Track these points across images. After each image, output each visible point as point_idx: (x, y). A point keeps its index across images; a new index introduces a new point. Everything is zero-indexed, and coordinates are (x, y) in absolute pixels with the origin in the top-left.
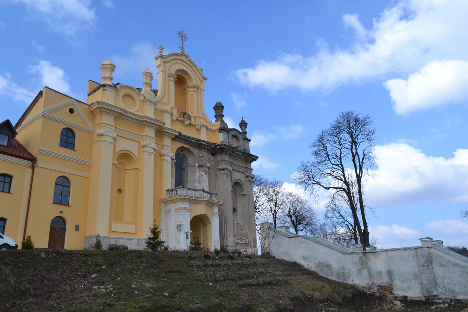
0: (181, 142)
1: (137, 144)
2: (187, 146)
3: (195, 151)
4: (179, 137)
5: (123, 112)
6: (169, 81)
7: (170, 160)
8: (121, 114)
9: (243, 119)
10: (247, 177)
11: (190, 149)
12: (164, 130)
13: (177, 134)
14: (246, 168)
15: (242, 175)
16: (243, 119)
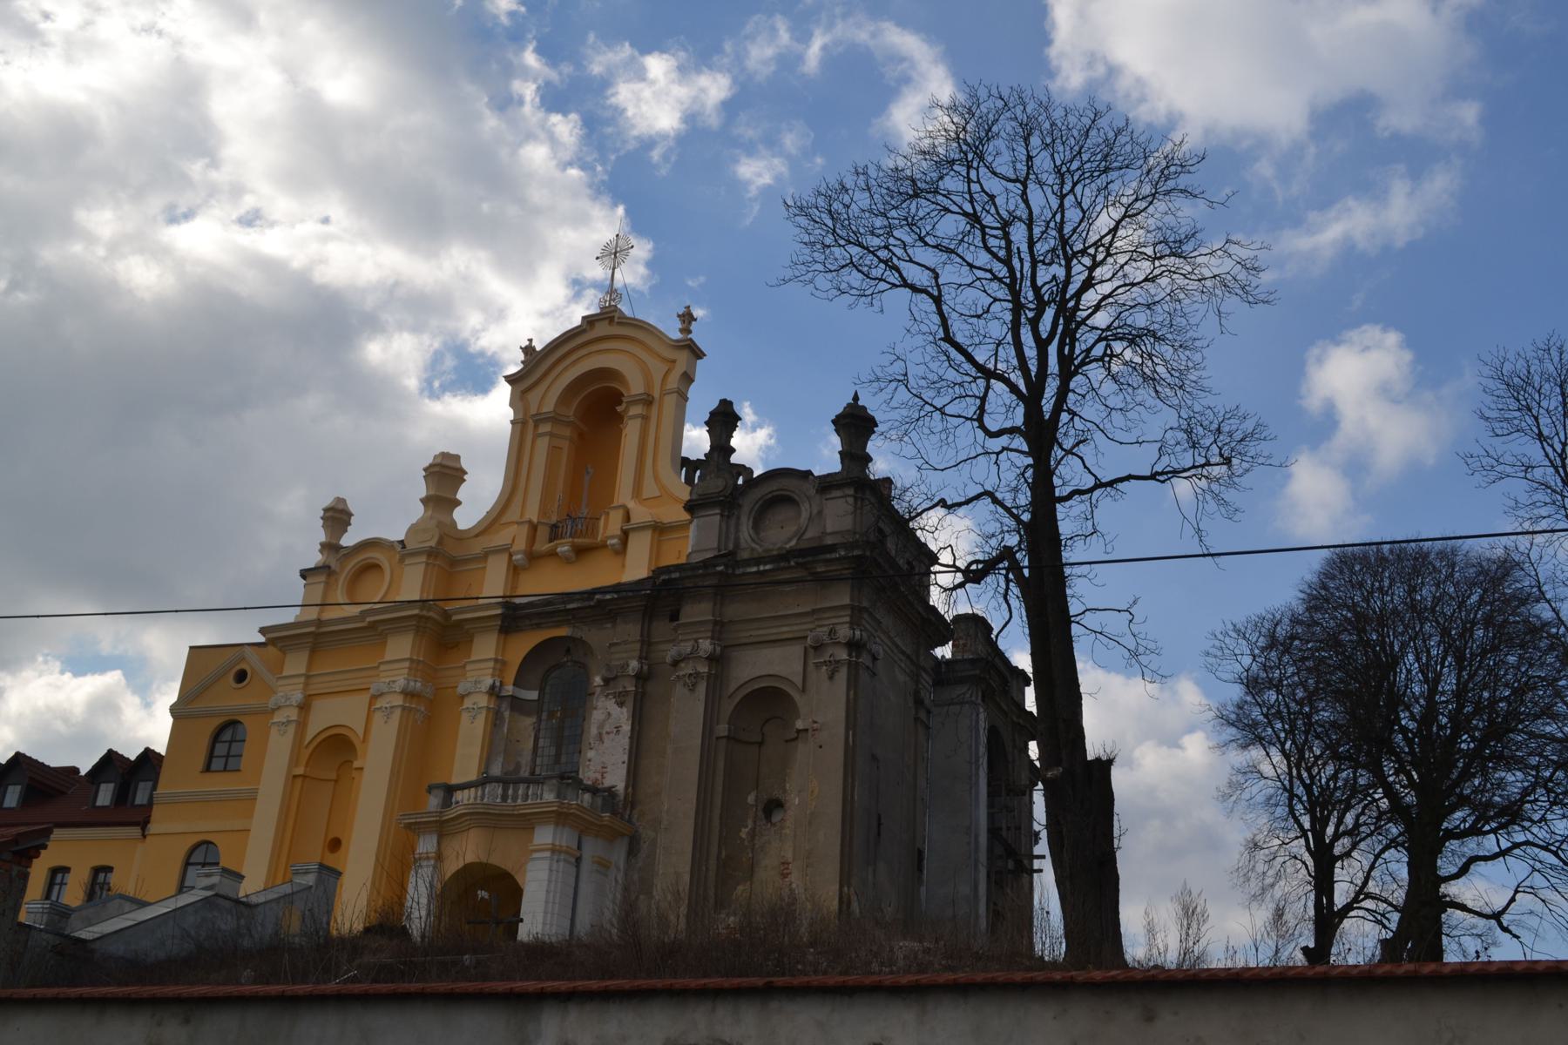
0: (538, 626)
1: (366, 697)
2: (563, 632)
3: (596, 637)
4: (513, 617)
5: (312, 629)
6: (536, 436)
7: (483, 701)
8: (315, 635)
9: (856, 398)
10: (816, 648)
11: (578, 634)
12: (455, 618)
13: (499, 611)
14: (814, 612)
15: (796, 650)
16: (856, 398)
